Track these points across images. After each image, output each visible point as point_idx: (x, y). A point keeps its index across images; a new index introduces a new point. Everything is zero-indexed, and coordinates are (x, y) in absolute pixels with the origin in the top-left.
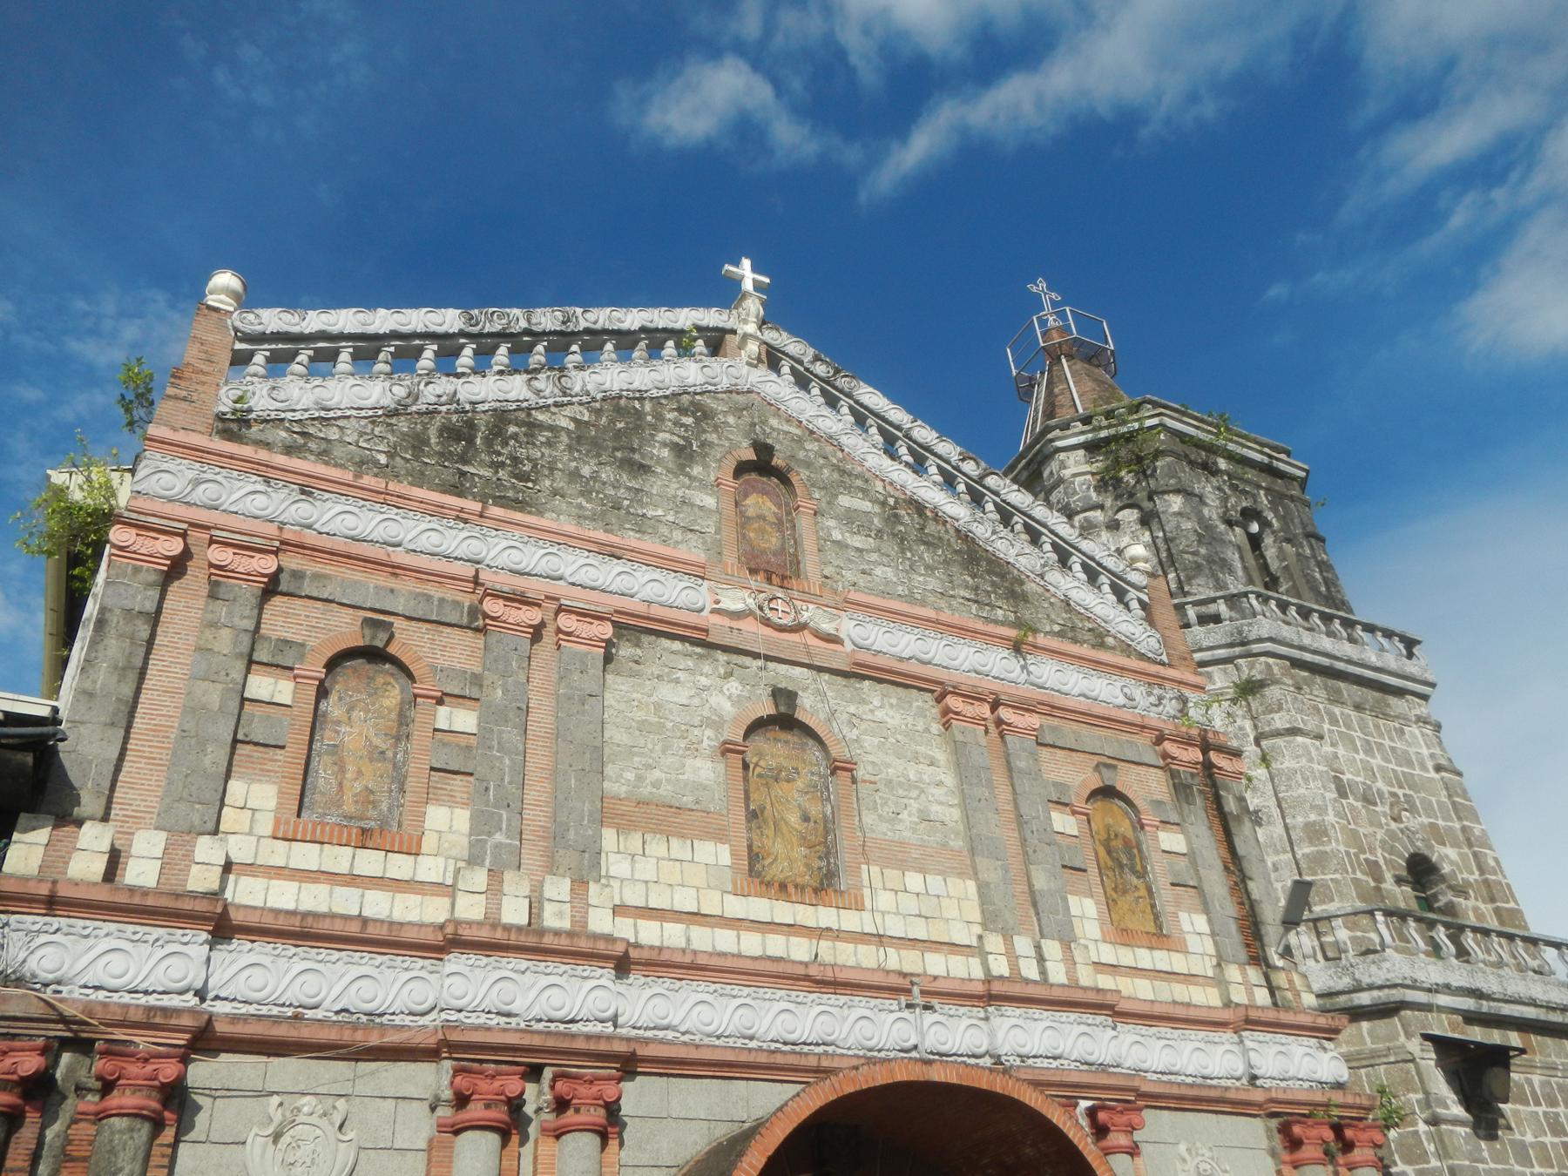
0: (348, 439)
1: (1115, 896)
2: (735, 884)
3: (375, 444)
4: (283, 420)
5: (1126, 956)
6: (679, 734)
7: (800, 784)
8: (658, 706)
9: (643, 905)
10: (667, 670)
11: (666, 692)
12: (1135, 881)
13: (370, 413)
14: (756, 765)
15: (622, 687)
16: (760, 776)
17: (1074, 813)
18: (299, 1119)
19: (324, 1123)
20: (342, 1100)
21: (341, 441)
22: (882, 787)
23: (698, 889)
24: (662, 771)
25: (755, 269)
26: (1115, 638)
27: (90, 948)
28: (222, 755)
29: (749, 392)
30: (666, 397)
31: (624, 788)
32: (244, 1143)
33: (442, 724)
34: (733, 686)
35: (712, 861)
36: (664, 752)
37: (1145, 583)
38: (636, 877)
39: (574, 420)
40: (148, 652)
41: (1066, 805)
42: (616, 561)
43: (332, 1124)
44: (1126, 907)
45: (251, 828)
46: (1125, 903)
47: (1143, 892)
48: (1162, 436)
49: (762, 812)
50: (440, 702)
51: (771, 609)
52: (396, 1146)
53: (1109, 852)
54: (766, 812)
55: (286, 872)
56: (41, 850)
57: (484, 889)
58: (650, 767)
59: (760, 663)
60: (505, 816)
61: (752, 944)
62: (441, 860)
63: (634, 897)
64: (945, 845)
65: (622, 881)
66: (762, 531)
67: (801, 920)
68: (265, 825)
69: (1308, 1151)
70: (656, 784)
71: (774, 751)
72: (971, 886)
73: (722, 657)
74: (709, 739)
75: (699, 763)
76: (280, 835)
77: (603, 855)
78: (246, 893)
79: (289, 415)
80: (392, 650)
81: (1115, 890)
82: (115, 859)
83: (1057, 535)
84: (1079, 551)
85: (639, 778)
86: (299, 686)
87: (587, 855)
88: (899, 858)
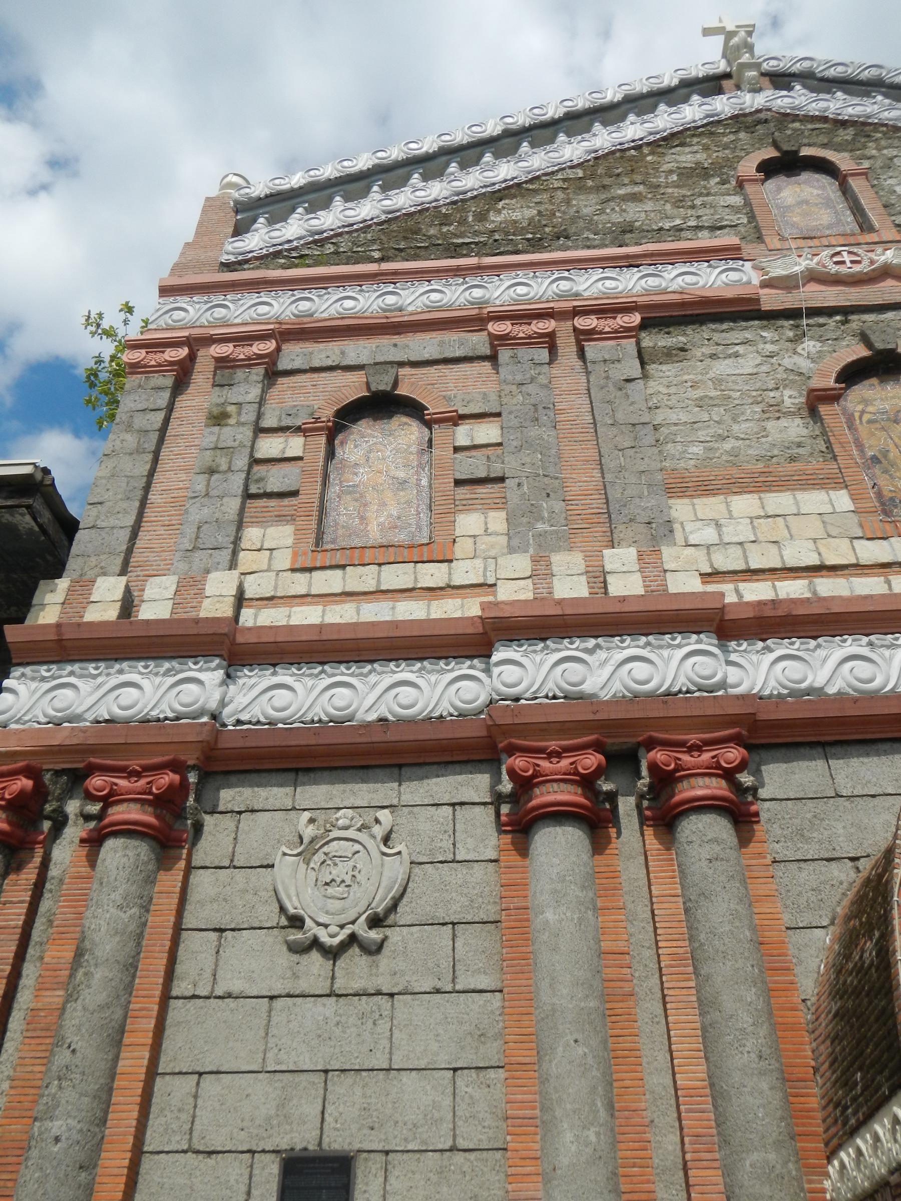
0: (342, 250)
3: (369, 246)
4: (280, 252)
6: (750, 401)
8: (718, 382)
9: (743, 567)
10: (721, 348)
13: (361, 225)
14: (863, 412)
15: (668, 373)
16: (870, 422)
18: (333, 835)
19: (362, 837)
20: (386, 811)
23: (815, 540)
24: (737, 438)
27: (100, 686)
28: (233, 505)
30: (664, 139)
31: (692, 462)
32: (272, 866)
33: (462, 441)
34: (810, 345)
35: (828, 509)
36: (734, 420)
38: (726, 540)
40: (161, 441)
42: (636, 269)
43: (373, 837)
45: (269, 565)
49: (885, 457)
50: (456, 425)
51: (837, 263)
52: (458, 858)
54: (891, 455)
55: (309, 599)
56: (59, 607)
57: (528, 574)
59: (838, 318)
60: (545, 505)
62: (478, 562)
65: (708, 547)
68: (284, 560)
70: (734, 453)
73: (787, 323)
74: (792, 398)
75: (783, 422)
76: (297, 566)
77: (677, 526)
79: (286, 246)
82: (128, 605)
86: (308, 439)
87: (654, 525)
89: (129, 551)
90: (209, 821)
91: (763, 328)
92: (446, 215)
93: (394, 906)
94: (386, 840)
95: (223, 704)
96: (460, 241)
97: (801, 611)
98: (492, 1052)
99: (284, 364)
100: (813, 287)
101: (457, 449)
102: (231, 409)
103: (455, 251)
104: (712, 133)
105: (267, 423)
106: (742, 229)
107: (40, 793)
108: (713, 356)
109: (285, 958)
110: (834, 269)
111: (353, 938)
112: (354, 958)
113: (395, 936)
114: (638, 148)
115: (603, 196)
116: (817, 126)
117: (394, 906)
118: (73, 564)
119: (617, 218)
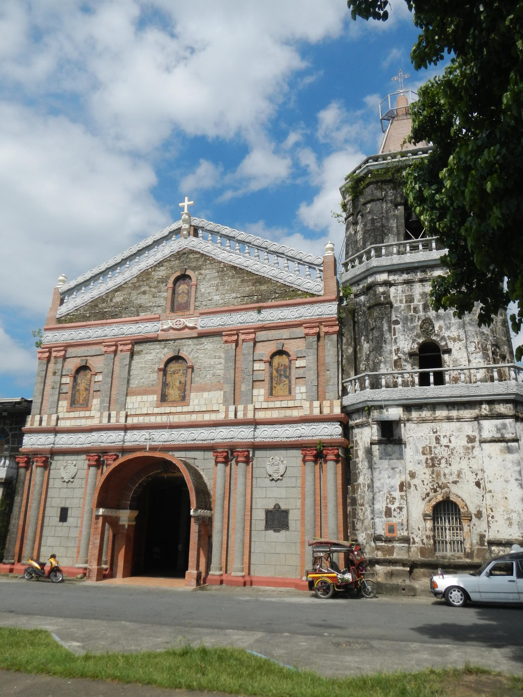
1: (276, 385)
2: (156, 404)
5: (271, 405)
7: (180, 374)
8: (146, 361)
11: (149, 357)
12: (285, 379)
17: (265, 362)
21: (80, 314)
22: (202, 369)
25: (189, 201)
26: (302, 291)
28: (56, 397)
29: (184, 249)
30: (158, 264)
34: (166, 350)
37: (321, 262)
39: (132, 283)
41: (262, 360)
44: (279, 388)
46: (278, 387)
47: (287, 382)
48: (369, 176)
50: (96, 375)
53: (277, 372)
58: (142, 379)
61: (159, 420)
63: (133, 412)
64: (219, 382)
66: (183, 296)
67: (172, 411)
68: (65, 410)
69: (308, 458)
70: (143, 383)
71: (173, 367)
72: (222, 392)
78: (62, 424)
79: (70, 312)
80: (88, 365)
81: (276, 384)
83: (288, 256)
84: (296, 259)
85: (139, 382)
88: (202, 389)
89: (41, 407)
90: (53, 462)
91: (158, 344)
92: (104, 299)
93: (75, 476)
94: (75, 466)
95: (55, 441)
96: (105, 310)
97: (138, 426)
98: (82, 496)
99: (67, 356)
100: (171, 331)
101: (95, 382)
102: (57, 371)
103: (103, 316)
104: (170, 260)
105: (64, 374)
106: (163, 307)
107: (29, 459)
108: (147, 353)
109: (62, 483)
110: (175, 327)
111: (69, 481)
112: (70, 483)
113: (75, 480)
114: (151, 268)
115: (139, 292)
116: (195, 256)
117: (75, 476)
118: (32, 413)
119: (139, 302)
